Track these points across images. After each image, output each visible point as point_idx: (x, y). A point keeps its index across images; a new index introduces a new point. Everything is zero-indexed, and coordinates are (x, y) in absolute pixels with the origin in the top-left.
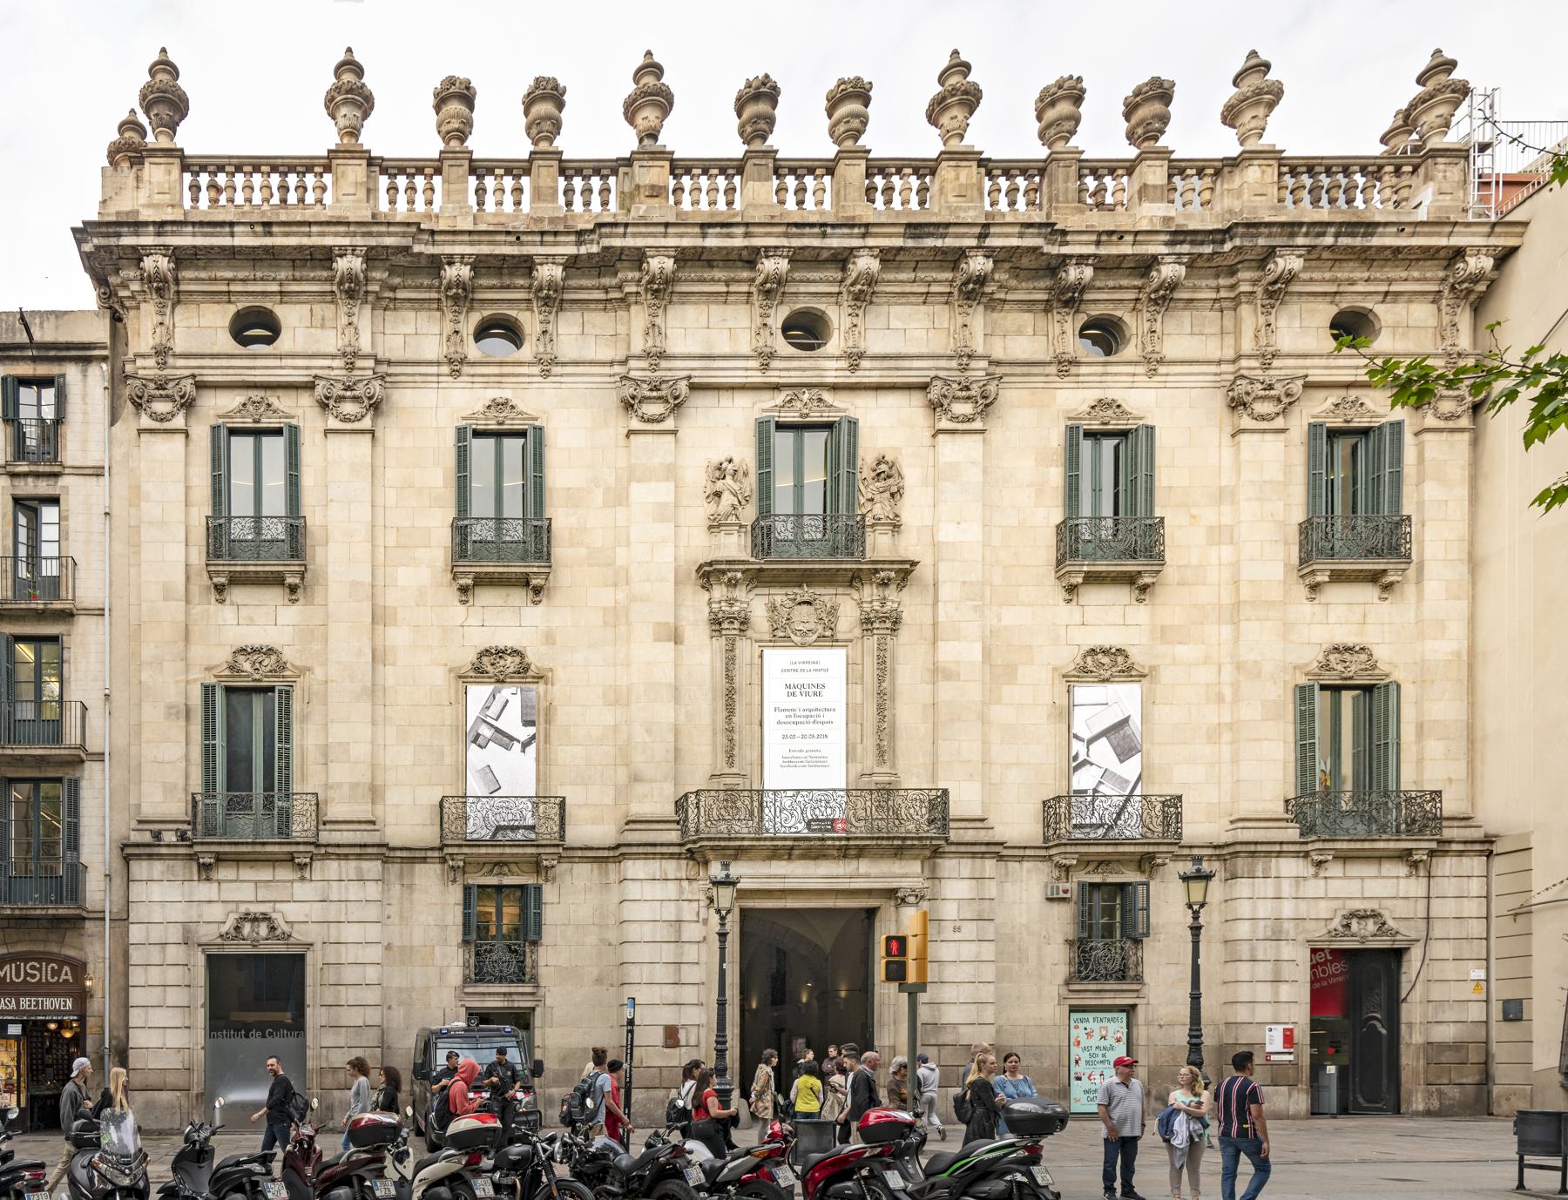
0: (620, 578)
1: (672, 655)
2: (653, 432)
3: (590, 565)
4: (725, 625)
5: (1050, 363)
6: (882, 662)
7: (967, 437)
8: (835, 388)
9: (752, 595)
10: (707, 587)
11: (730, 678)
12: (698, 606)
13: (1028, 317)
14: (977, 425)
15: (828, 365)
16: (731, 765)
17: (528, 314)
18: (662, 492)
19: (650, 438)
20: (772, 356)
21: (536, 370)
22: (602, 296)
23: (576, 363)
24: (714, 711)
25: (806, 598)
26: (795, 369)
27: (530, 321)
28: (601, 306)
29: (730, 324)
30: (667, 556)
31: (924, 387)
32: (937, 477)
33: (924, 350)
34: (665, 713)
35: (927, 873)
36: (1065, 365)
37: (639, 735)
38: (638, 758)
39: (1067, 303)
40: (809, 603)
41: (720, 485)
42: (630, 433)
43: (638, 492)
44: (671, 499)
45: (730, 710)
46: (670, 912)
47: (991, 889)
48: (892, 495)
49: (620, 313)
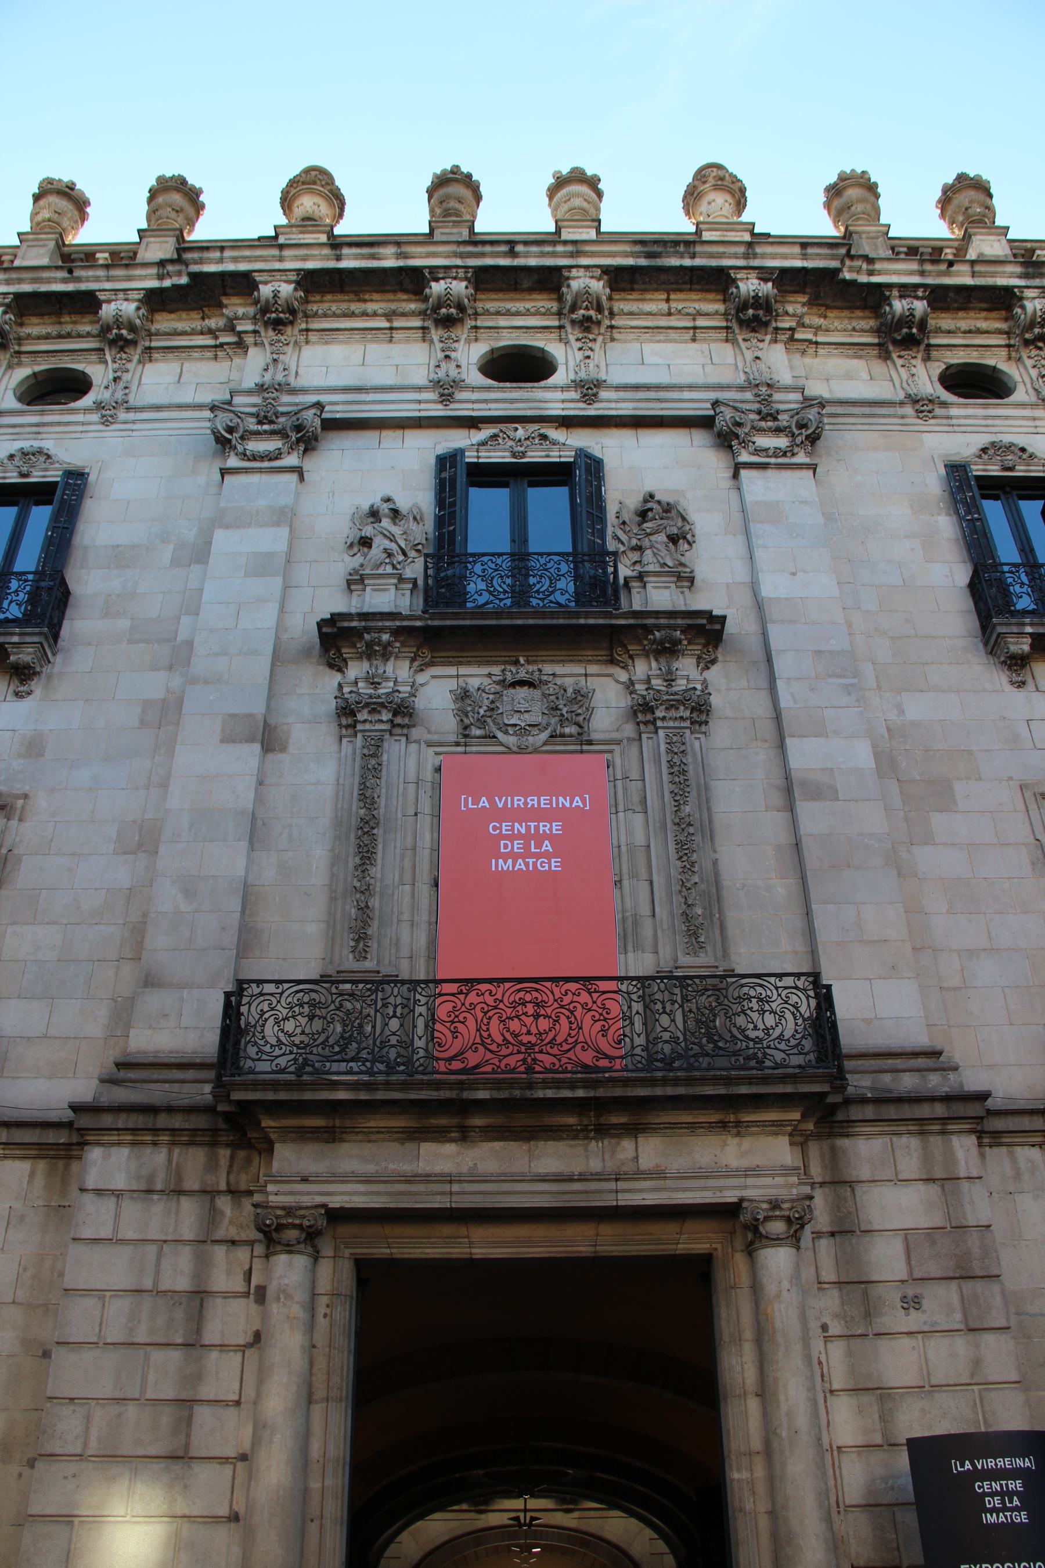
0: (180, 656)
1: (254, 763)
2: (260, 470)
3: (131, 642)
4: (363, 715)
5: (902, 404)
6: (678, 772)
7: (787, 474)
8: (567, 422)
9: (421, 678)
10: (337, 665)
11: (367, 798)
12: (317, 690)
13: (855, 362)
14: (801, 458)
15: (552, 397)
16: (362, 955)
17: (101, 368)
18: (273, 540)
19: (255, 479)
20: (457, 384)
21: (95, 417)
22: (211, 342)
23: (158, 408)
24: (335, 860)
25: (522, 675)
26: (496, 401)
27: (98, 373)
28: (209, 354)
29: (396, 361)
30: (267, 617)
31: (705, 423)
32: (745, 524)
33: (700, 380)
34: (229, 860)
35: (816, 1171)
36: (922, 406)
37: (167, 898)
38: (158, 941)
39: (910, 342)
40: (530, 684)
41: (368, 531)
42: (224, 472)
43: (222, 540)
44: (282, 546)
45: (366, 855)
46: (178, 1276)
47: (978, 1206)
48: (674, 539)
49: (237, 361)
